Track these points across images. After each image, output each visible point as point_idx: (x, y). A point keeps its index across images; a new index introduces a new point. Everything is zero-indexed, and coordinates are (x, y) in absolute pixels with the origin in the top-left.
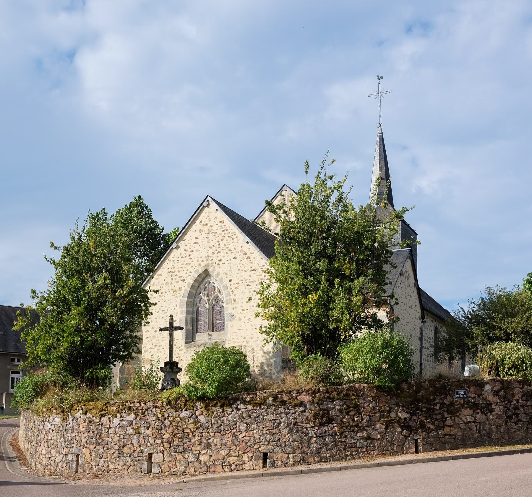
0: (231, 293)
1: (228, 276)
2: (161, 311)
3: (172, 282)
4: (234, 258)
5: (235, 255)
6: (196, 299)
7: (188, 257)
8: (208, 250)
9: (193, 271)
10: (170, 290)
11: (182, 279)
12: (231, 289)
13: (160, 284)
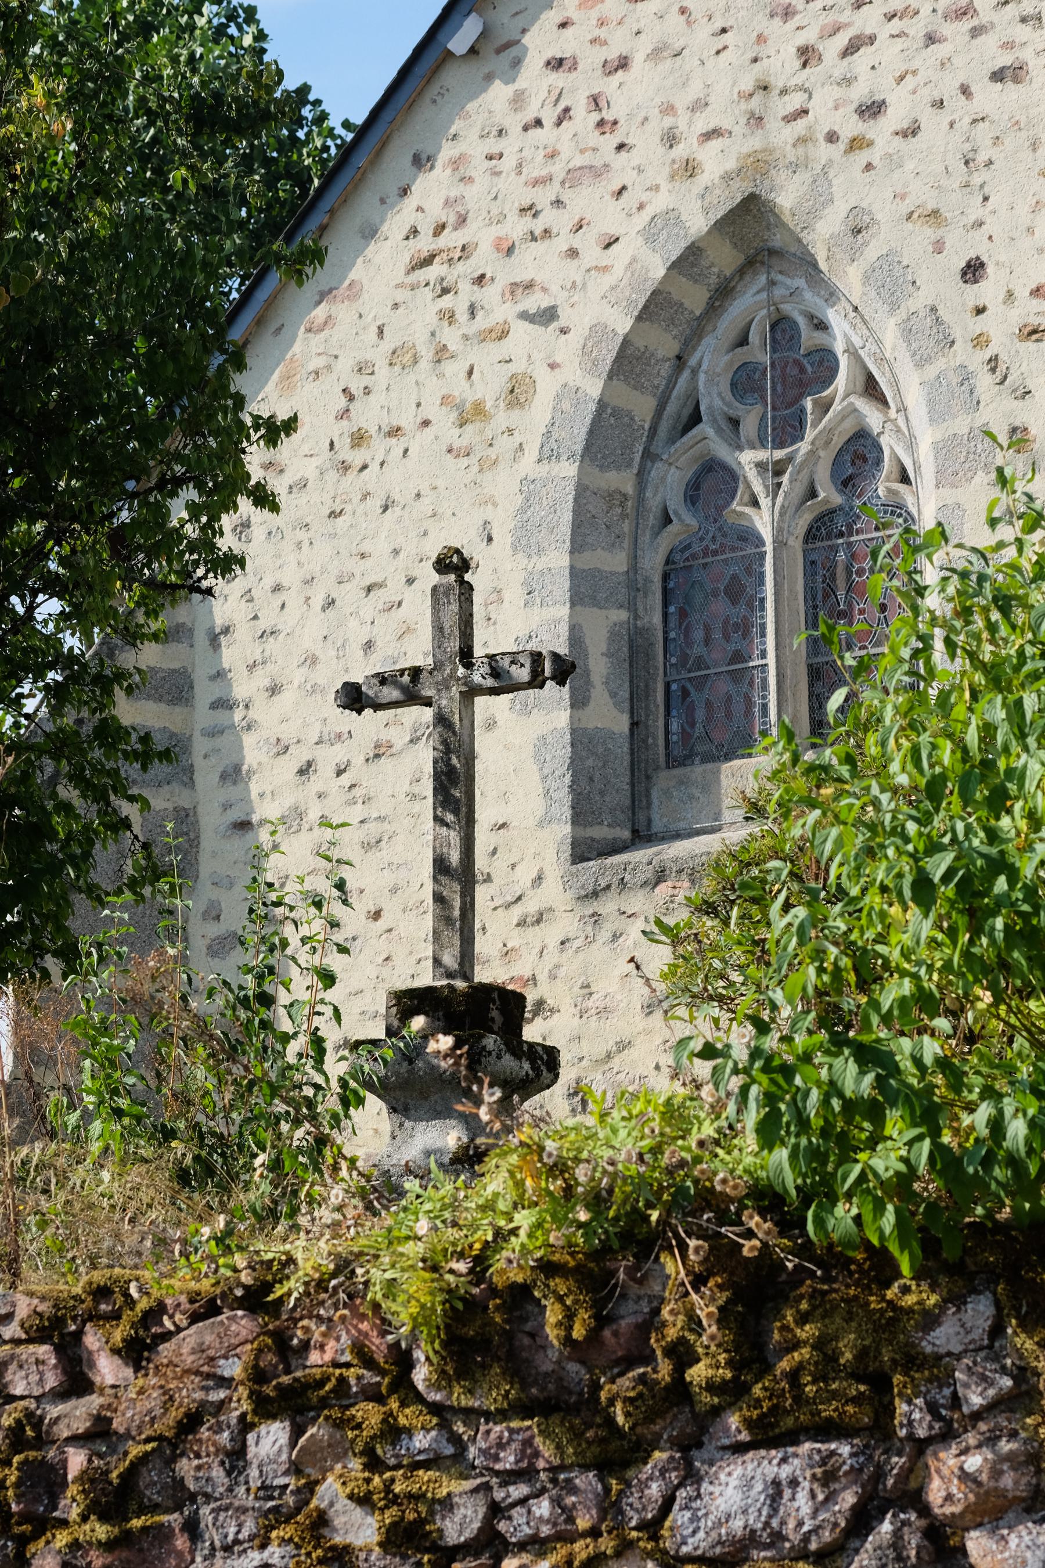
0: (985, 382)
1: (953, 237)
2: (349, 595)
3: (450, 337)
4: (998, 76)
5: (1008, 46)
6: (656, 471)
7: (583, 119)
8: (761, 39)
9: (631, 229)
10: (432, 410)
11: (534, 302)
12: (980, 341)
13: (345, 365)
